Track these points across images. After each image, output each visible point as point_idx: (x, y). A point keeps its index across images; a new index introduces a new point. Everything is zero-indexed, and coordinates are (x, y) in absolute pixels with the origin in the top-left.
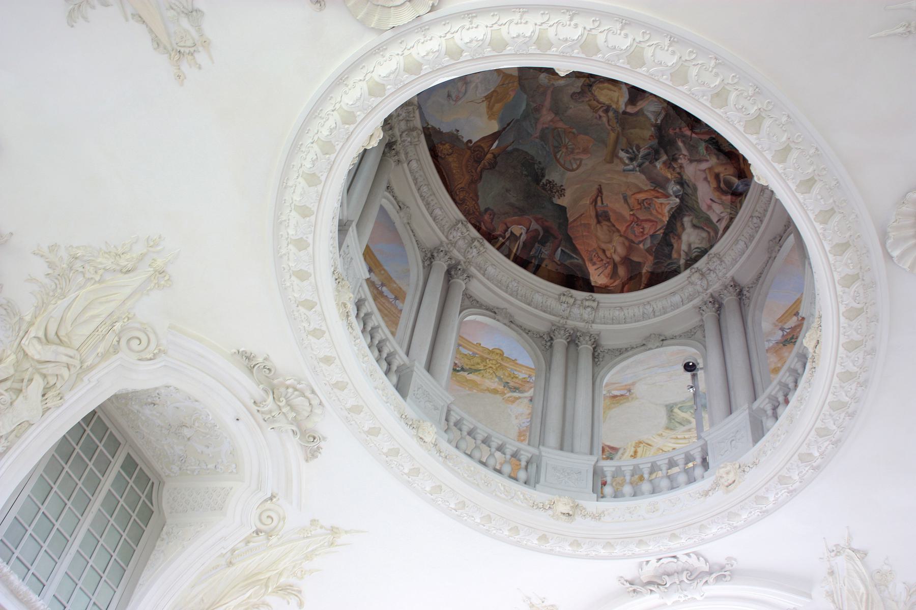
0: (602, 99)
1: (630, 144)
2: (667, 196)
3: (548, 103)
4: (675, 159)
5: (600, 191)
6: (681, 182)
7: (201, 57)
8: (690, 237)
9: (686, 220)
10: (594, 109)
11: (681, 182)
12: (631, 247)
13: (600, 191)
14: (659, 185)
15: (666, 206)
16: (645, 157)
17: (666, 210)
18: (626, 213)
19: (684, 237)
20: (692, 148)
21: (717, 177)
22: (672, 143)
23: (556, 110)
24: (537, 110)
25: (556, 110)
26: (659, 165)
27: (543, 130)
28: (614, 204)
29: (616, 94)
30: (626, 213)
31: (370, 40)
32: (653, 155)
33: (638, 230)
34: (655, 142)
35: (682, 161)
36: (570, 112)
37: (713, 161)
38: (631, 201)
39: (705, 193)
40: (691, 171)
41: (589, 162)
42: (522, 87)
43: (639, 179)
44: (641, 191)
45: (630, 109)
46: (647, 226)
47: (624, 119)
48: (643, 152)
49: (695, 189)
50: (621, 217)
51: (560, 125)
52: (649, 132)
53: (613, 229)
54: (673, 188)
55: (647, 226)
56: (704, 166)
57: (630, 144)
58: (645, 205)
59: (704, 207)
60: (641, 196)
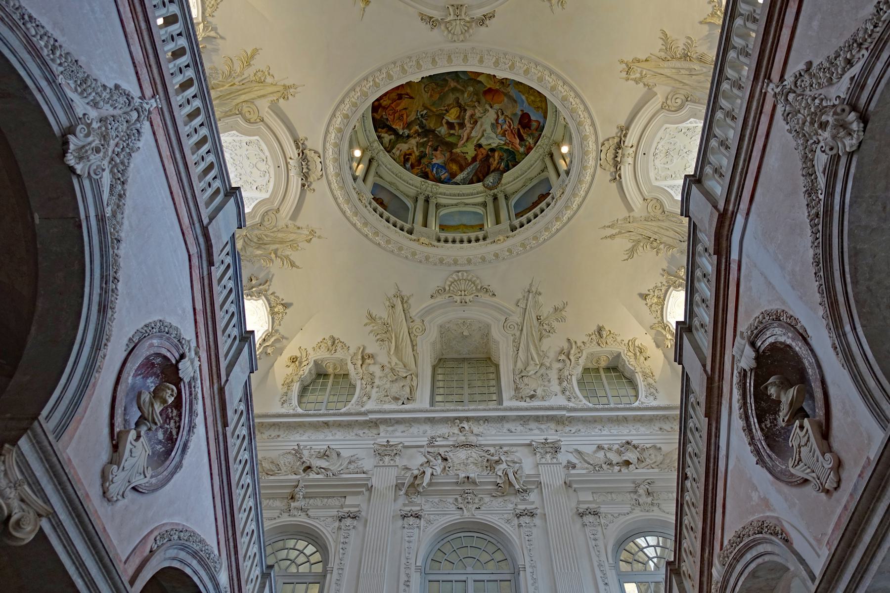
0: (452, 110)
1: (429, 116)
2: (403, 129)
3: (459, 87)
4: (419, 135)
5: (411, 98)
6: (409, 137)
7: (624, 74)
8: (387, 137)
9: (393, 137)
10: (448, 106)
11: (409, 137)
12: (385, 108)
13: (411, 98)
14: (408, 126)
15: (399, 127)
16: (422, 122)
17: (398, 127)
18: (399, 108)
19: (386, 135)
20: (424, 145)
21: (410, 154)
22: (426, 136)
23: (454, 90)
24: (458, 82)
25: (454, 90)
26: (417, 127)
27: (447, 81)
28: (404, 103)
29: (452, 117)
30: (399, 108)
31: (601, 141)
32: (422, 126)
33: (391, 112)
34: (428, 128)
35: (418, 139)
36: (451, 94)
37: (417, 153)
38: (404, 112)
39: (403, 147)
40: (413, 142)
41: (426, 96)
42: (471, 79)
43: (412, 117)
44: (407, 116)
45: (444, 121)
46: (392, 117)
47: (441, 117)
48: (424, 121)
49: (406, 143)
50: (398, 105)
51: (447, 89)
52: (432, 126)
53: (394, 101)
54: (407, 132)
55: (392, 117)
56: (415, 149)
57: (429, 116)
58: (401, 118)
59: (398, 146)
60: (405, 116)
